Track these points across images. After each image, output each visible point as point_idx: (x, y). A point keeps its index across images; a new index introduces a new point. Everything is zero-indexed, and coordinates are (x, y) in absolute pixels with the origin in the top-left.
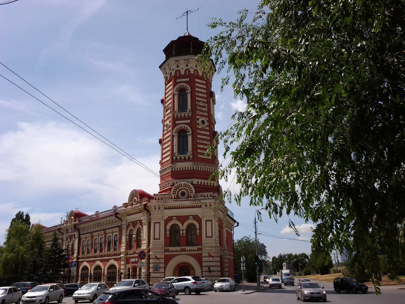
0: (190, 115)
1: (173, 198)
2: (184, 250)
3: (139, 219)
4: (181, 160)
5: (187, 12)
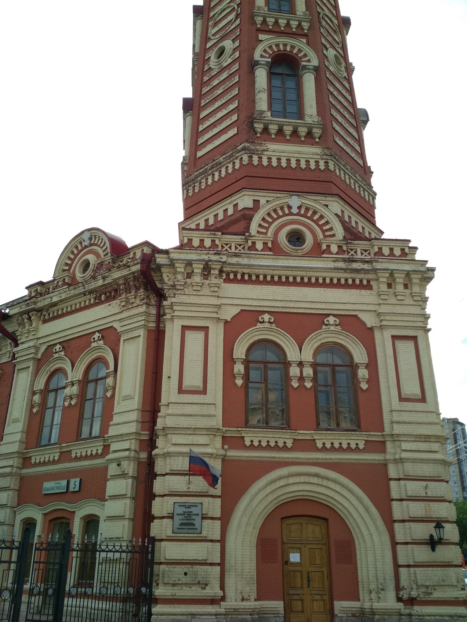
0: (305, 25)
1: (259, 246)
2: (309, 445)
3: (102, 324)
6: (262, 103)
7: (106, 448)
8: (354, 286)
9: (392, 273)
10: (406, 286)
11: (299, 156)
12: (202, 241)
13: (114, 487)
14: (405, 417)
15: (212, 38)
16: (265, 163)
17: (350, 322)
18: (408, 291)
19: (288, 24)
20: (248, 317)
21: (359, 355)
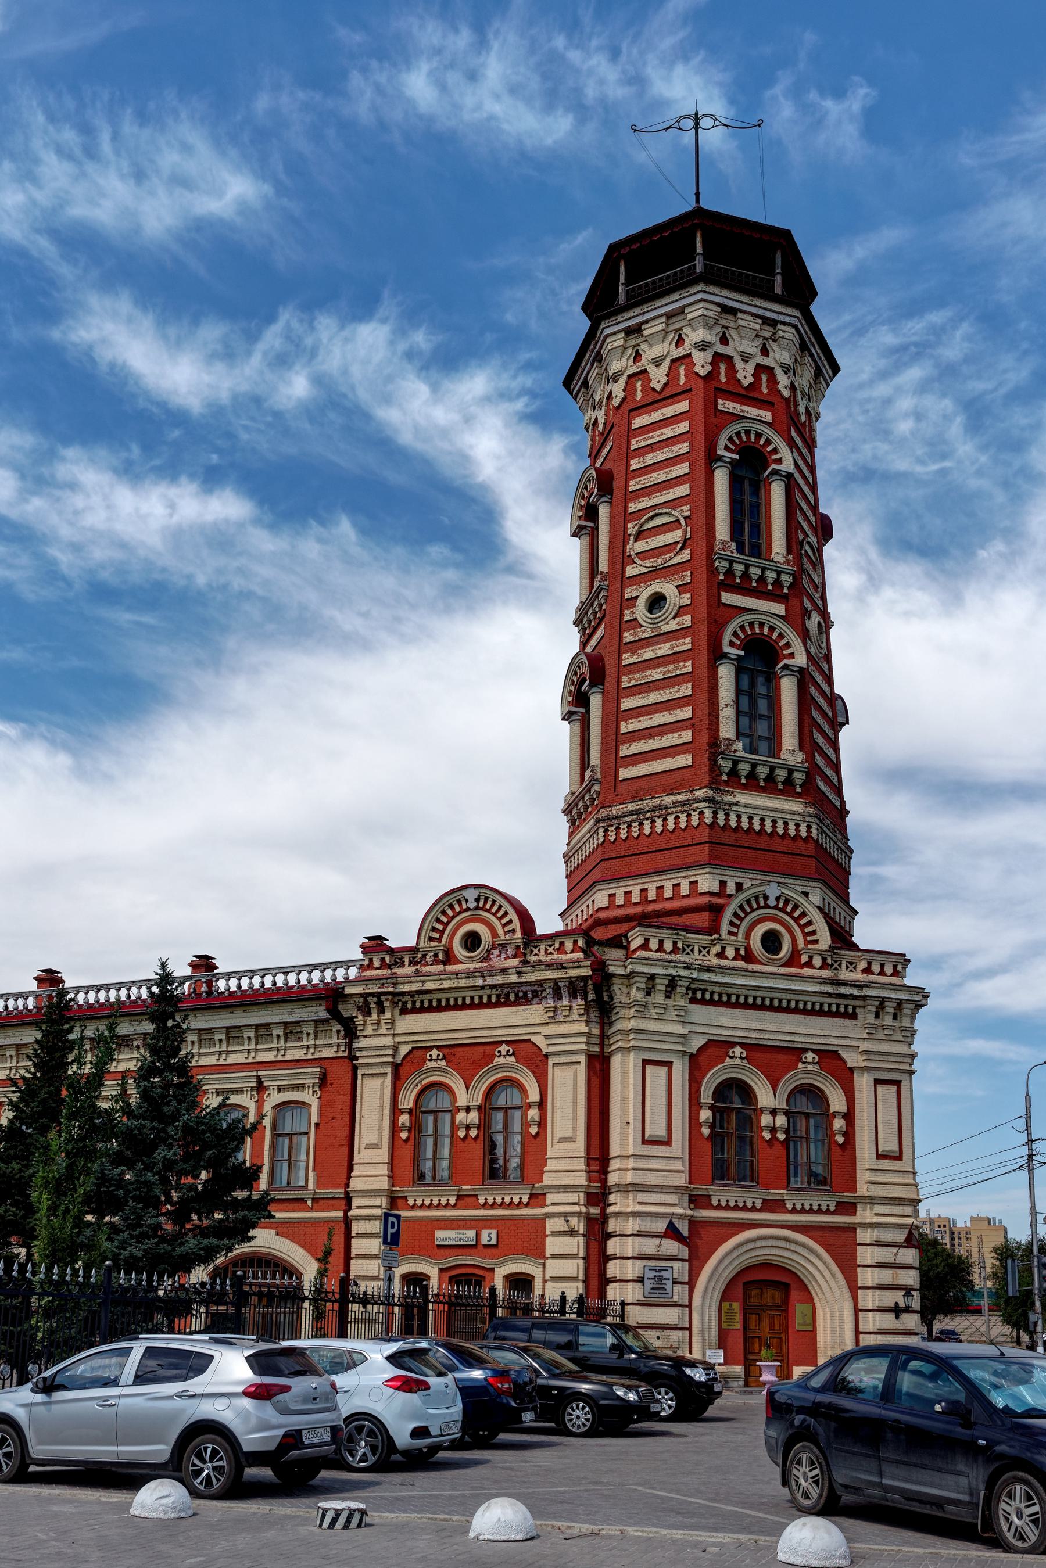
0: (786, 579)
1: (730, 952)
4: (752, 783)
7: (537, 1198)
8: (837, 1015)
10: (895, 1017)
11: (775, 815)
12: (661, 942)
13: (552, 1245)
15: (637, 560)
17: (830, 1059)
21: (837, 1102)
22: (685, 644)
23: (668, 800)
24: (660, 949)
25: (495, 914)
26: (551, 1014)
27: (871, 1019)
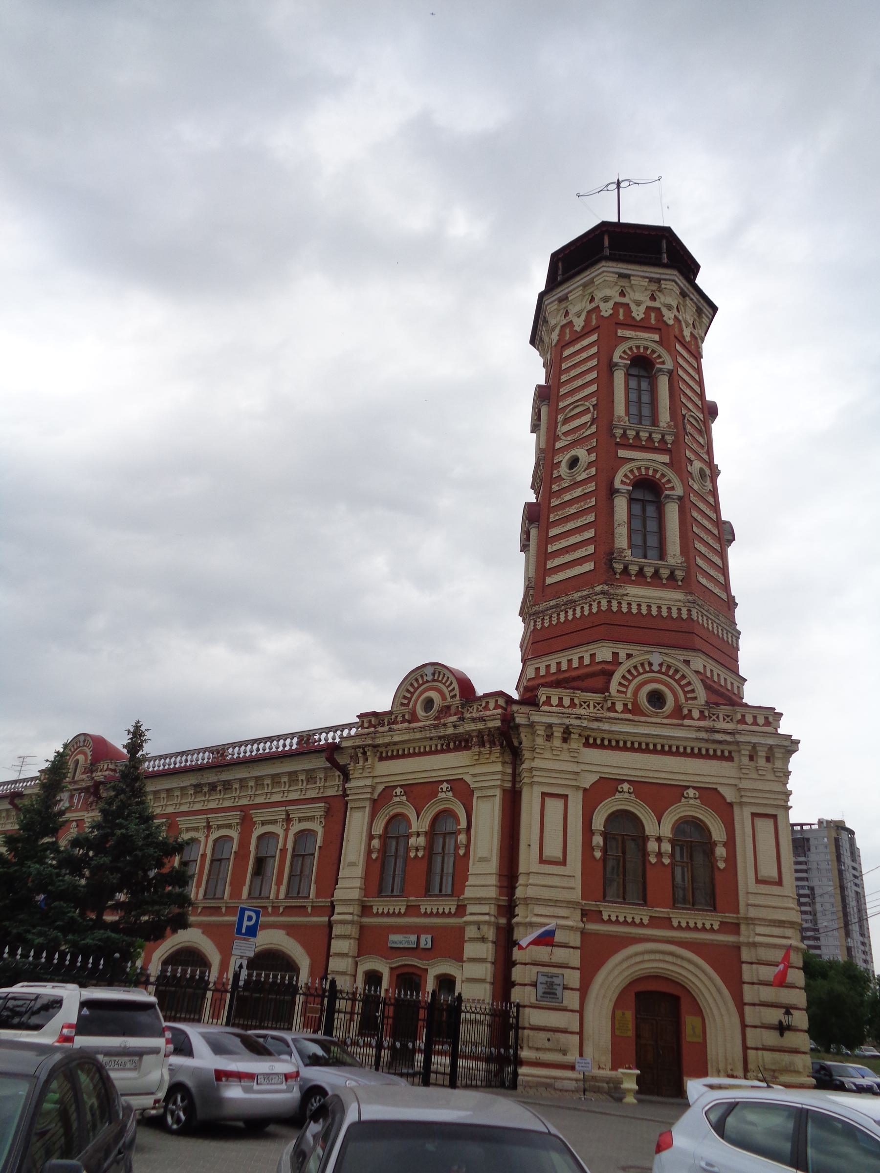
0: (669, 438)
1: (619, 707)
2: (666, 923)
5: (618, 184)
6: (621, 540)
7: (461, 910)
8: (715, 757)
9: (754, 746)
10: (768, 759)
12: (561, 699)
13: (470, 950)
14: (760, 901)
15: (563, 437)
16: (625, 610)
17: (710, 795)
18: (769, 765)
19: (650, 438)
20: (606, 786)
21: (718, 833)
22: (591, 487)
23: (576, 596)
24: (560, 704)
25: (444, 684)
26: (477, 757)
27: (745, 760)
